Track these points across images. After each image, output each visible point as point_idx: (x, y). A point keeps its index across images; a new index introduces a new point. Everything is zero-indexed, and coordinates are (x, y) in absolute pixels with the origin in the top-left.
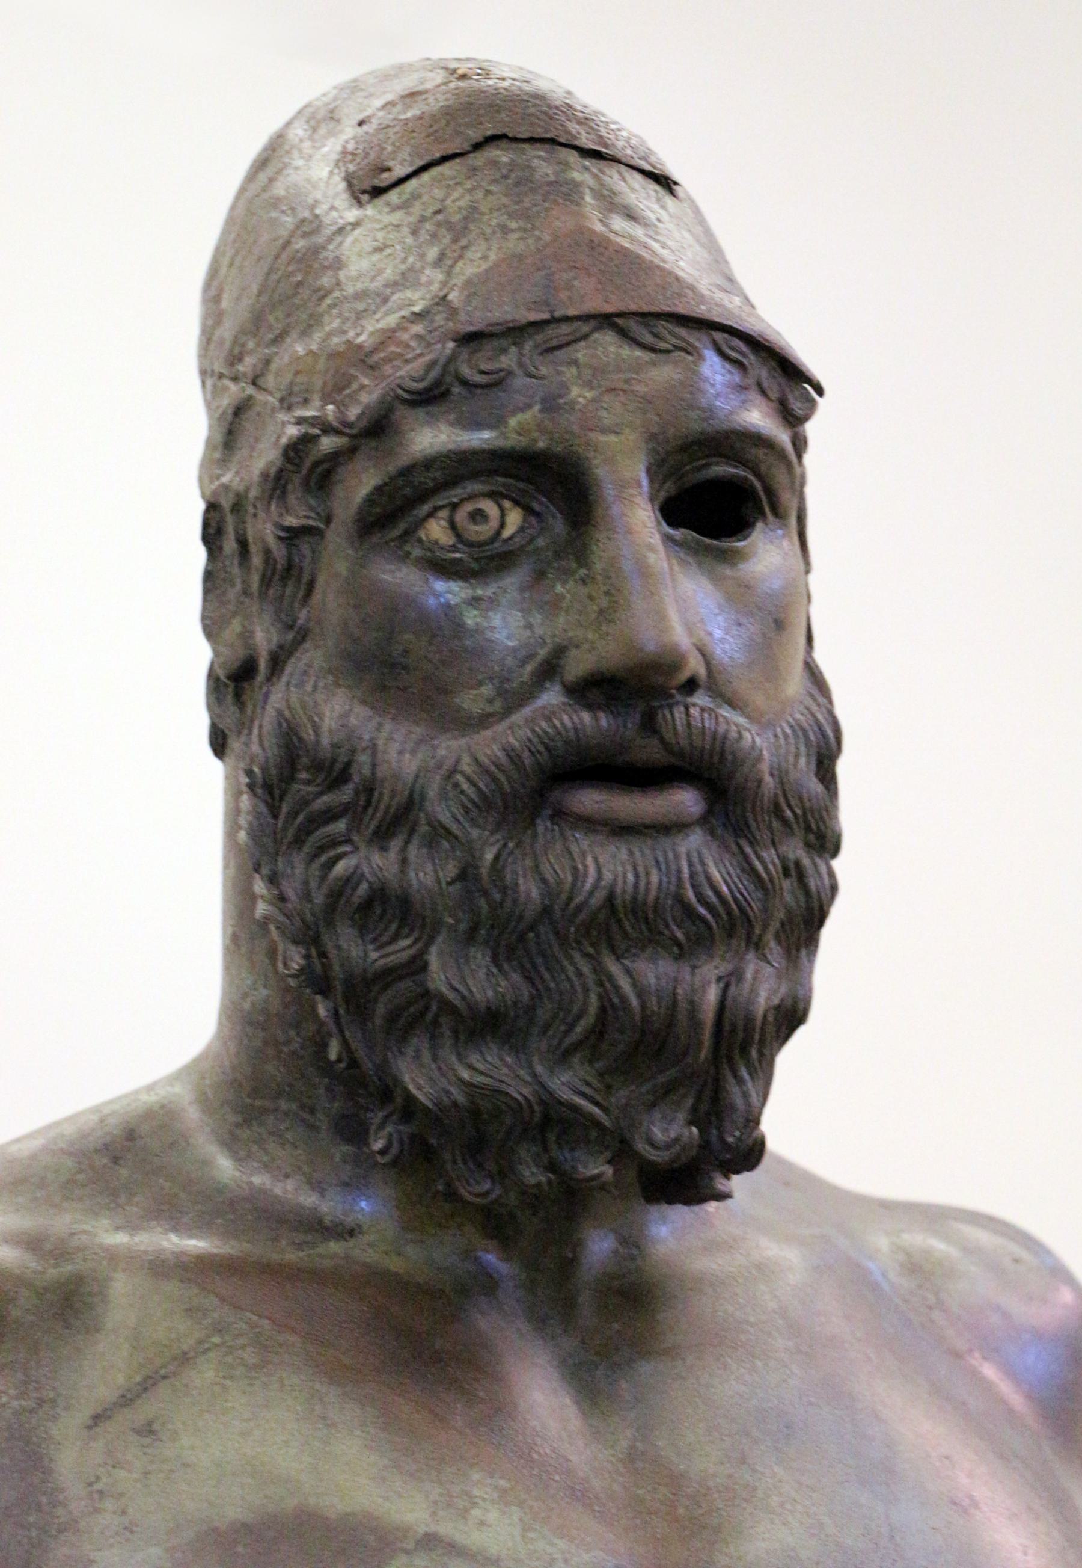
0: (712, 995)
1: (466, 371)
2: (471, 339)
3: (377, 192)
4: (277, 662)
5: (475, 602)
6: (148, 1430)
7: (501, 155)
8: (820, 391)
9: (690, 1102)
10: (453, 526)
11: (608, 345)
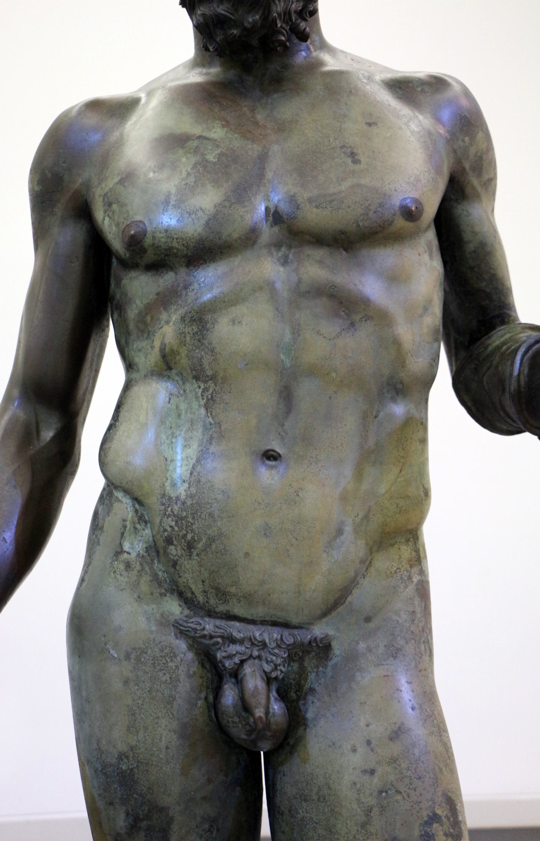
9: (261, 12)
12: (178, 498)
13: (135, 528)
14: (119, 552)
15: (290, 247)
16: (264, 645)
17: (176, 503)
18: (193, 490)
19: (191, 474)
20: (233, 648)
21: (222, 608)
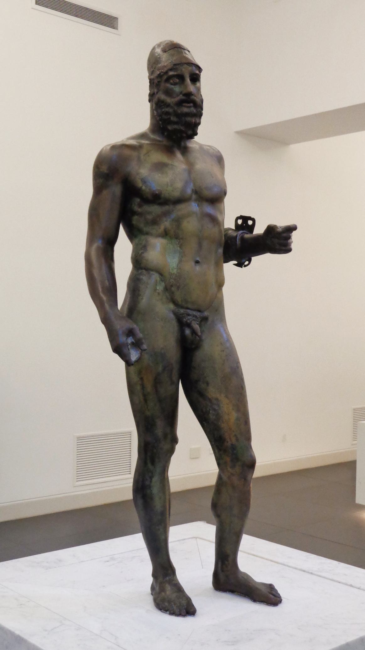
0: (194, 121)
1: (174, 68)
2: (175, 65)
3: (165, 52)
4: (157, 93)
5: (175, 87)
6: (149, 156)
7: (176, 49)
8: (202, 70)
10: (173, 81)
11: (186, 66)
12: (174, 274)
13: (160, 283)
14: (155, 290)
15: (199, 201)
16: (196, 317)
17: (174, 275)
18: (179, 271)
19: (177, 266)
20: (189, 317)
21: (185, 306)
